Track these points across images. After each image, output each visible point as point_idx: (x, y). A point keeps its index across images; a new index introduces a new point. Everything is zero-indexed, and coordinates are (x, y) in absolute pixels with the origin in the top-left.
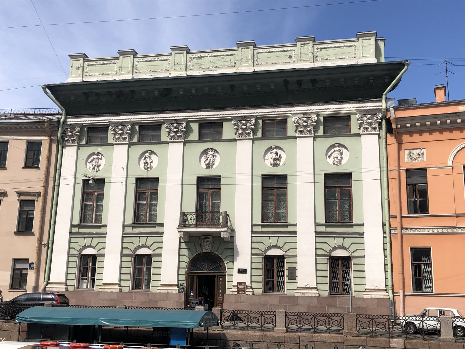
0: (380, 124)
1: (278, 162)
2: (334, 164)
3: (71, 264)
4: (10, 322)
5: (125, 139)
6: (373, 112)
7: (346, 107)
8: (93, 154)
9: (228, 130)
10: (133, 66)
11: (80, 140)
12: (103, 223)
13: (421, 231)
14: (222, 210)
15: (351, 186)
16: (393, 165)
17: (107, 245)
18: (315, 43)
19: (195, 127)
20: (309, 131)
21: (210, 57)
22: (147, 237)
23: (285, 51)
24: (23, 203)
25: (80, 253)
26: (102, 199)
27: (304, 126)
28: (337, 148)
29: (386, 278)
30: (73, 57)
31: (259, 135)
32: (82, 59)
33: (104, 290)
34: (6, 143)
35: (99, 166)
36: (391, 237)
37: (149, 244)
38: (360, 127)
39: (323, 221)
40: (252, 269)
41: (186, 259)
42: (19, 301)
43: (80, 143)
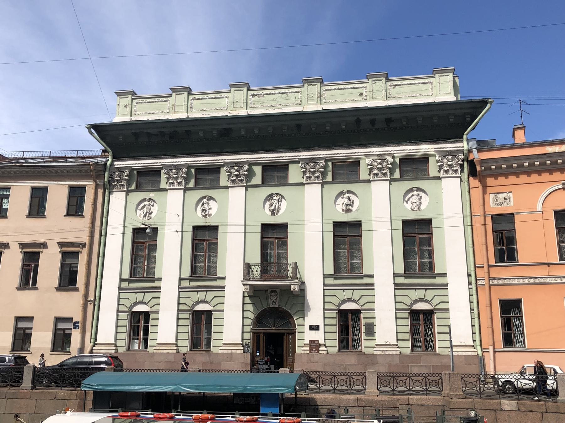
0: (462, 166)
1: (350, 207)
2: (413, 210)
3: (121, 323)
4: (64, 390)
5: (180, 183)
6: (453, 154)
7: (423, 149)
8: (144, 200)
9: (295, 174)
10: (188, 104)
11: (129, 185)
12: (156, 276)
13: (511, 282)
14: (291, 260)
15: (432, 234)
16: (478, 210)
17: (161, 301)
18: (388, 80)
19: (258, 170)
20: (385, 174)
21: (273, 94)
23: (355, 88)
24: (65, 255)
25: (131, 310)
26: (155, 250)
27: (378, 168)
28: (415, 193)
29: (473, 333)
31: (329, 178)
32: (130, 96)
33: (159, 351)
34: (46, 189)
35: (150, 214)
36: (477, 288)
37: (208, 299)
38: (440, 170)
39: (402, 272)
40: (325, 325)
41: (252, 316)
42: (67, 365)
43: (130, 189)
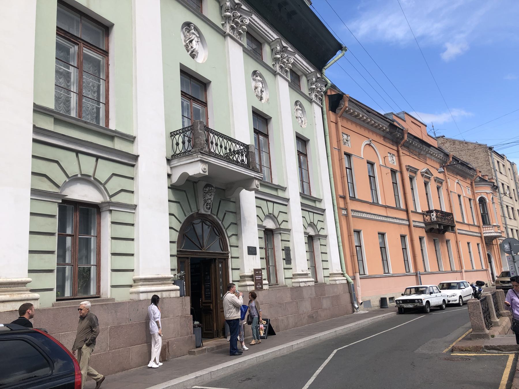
22: (98, 157)
37: (102, 175)
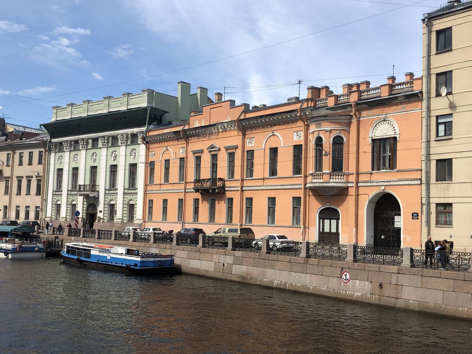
19: (90, 141)
30: (53, 108)
41: (85, 206)
